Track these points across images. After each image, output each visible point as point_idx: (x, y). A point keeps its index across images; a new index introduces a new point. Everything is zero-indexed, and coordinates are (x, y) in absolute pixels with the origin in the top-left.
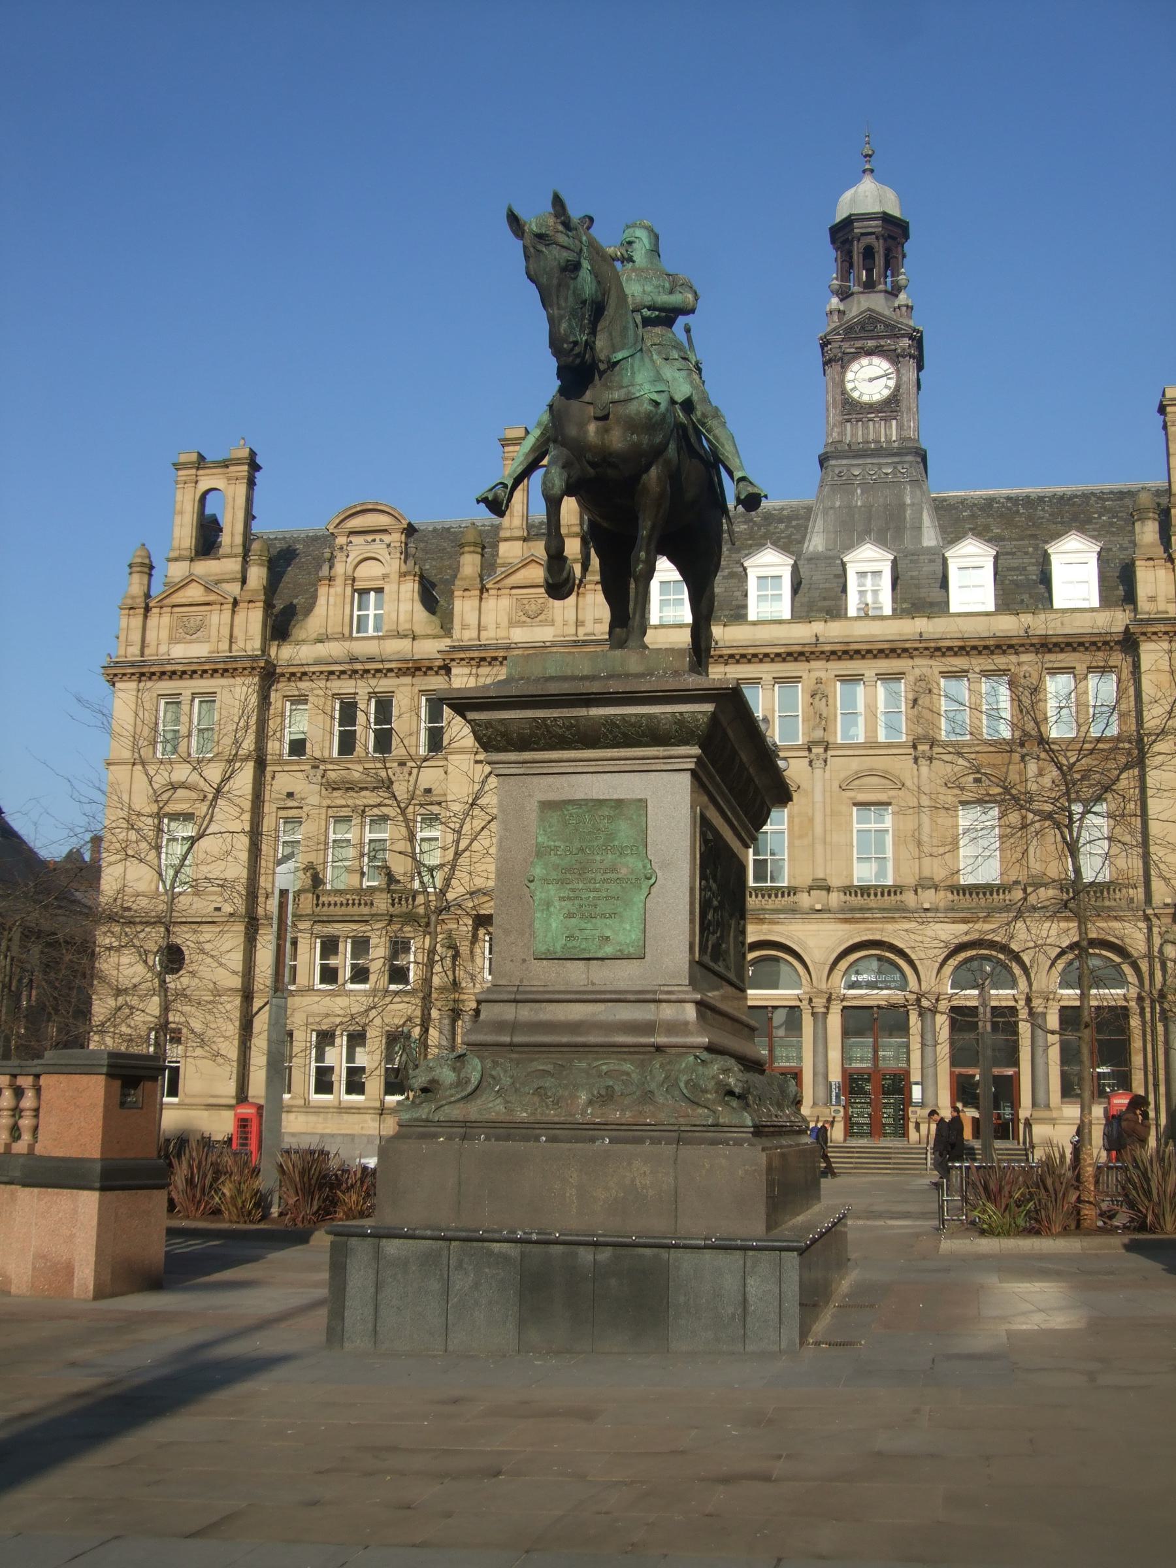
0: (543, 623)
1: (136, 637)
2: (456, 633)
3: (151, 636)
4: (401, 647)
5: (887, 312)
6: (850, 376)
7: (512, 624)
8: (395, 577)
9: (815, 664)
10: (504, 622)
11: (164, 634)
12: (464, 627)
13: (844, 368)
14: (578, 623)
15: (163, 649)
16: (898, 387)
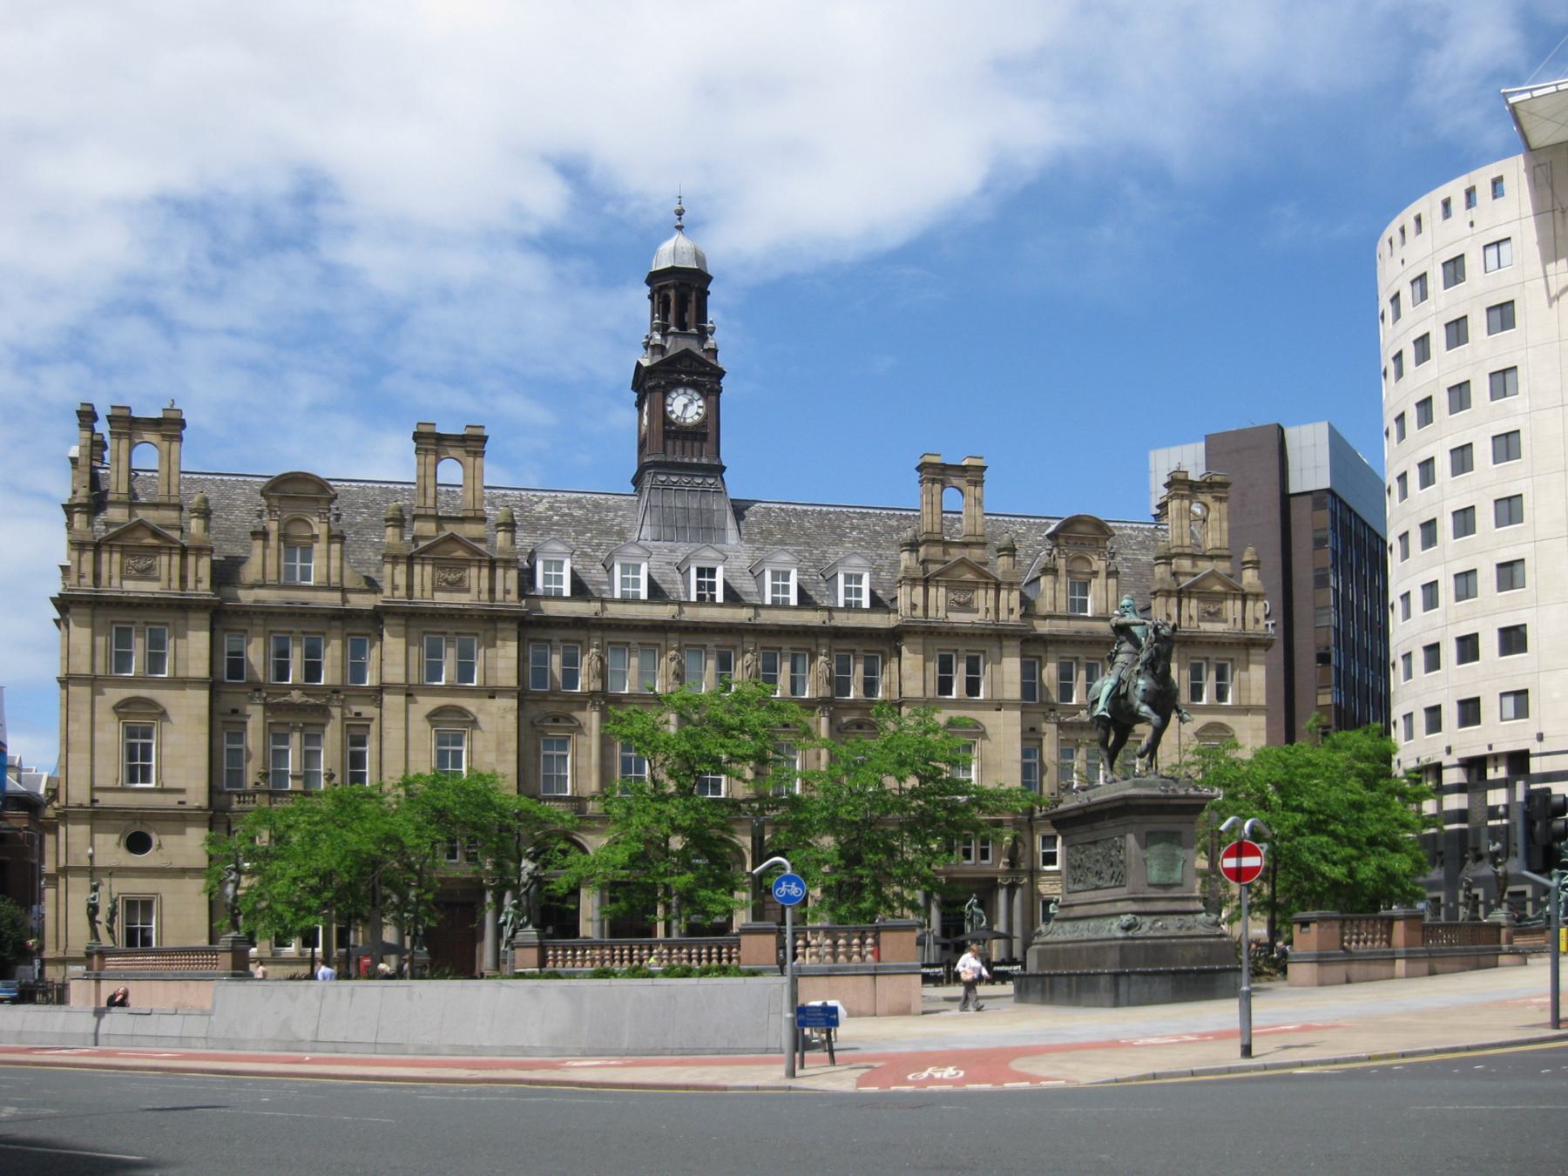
0: (460, 591)
1: (87, 568)
2: (387, 592)
3: (104, 569)
4: (332, 599)
5: (699, 352)
6: (669, 401)
7: (435, 589)
8: (323, 538)
9: (670, 635)
10: (428, 585)
11: (116, 569)
12: (395, 588)
13: (665, 395)
14: (492, 590)
15: (116, 582)
16: (706, 416)
